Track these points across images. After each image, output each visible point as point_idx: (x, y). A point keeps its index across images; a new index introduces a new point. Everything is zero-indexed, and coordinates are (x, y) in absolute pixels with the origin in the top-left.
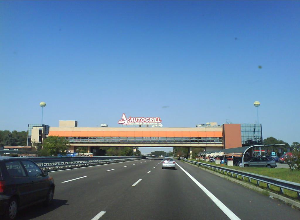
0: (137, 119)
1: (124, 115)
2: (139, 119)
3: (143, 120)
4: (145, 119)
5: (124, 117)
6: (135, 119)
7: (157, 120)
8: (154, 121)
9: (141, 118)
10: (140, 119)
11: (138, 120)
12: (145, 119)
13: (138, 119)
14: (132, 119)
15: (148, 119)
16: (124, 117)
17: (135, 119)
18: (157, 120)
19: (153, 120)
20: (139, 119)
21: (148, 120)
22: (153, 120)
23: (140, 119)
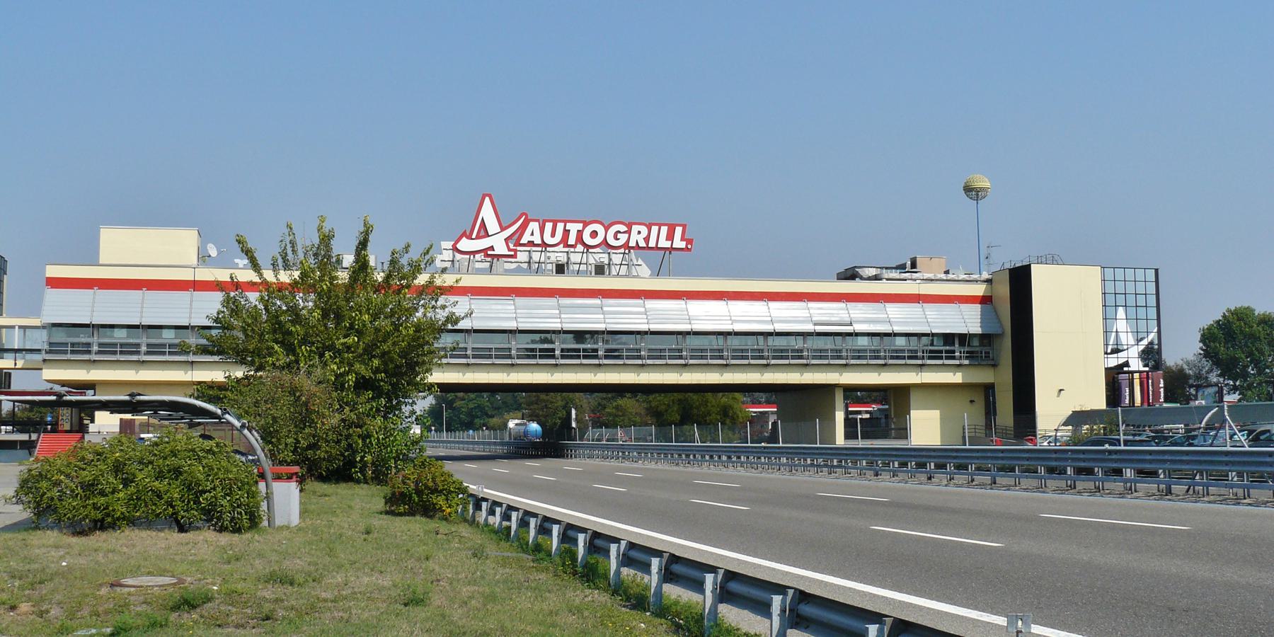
0: (560, 226)
1: (487, 199)
2: (574, 228)
3: (594, 234)
4: (607, 229)
5: (487, 213)
6: (549, 226)
7: (670, 237)
8: (652, 244)
9: (586, 224)
10: (580, 226)
11: (566, 232)
12: (607, 229)
13: (569, 226)
14: (534, 226)
15: (623, 228)
16: (487, 213)
17: (549, 226)
18: (670, 237)
19: (647, 239)
20: (574, 228)
21: (623, 238)
22: (647, 239)
23: (580, 226)
